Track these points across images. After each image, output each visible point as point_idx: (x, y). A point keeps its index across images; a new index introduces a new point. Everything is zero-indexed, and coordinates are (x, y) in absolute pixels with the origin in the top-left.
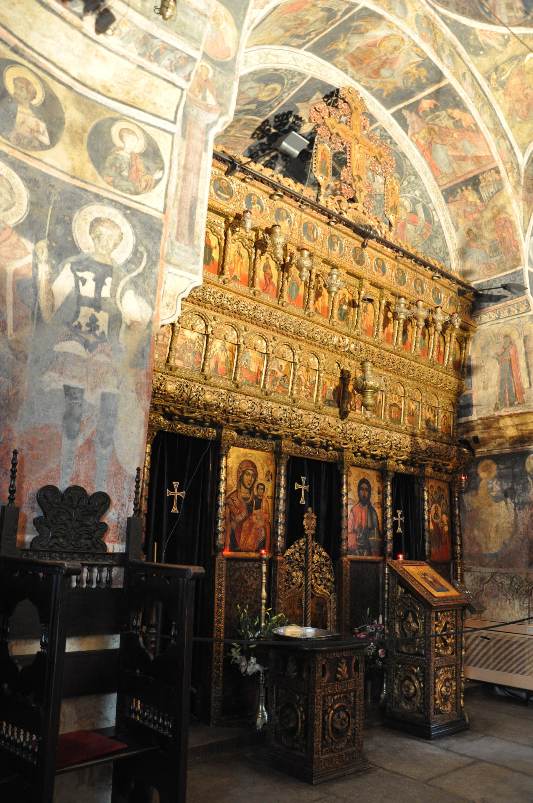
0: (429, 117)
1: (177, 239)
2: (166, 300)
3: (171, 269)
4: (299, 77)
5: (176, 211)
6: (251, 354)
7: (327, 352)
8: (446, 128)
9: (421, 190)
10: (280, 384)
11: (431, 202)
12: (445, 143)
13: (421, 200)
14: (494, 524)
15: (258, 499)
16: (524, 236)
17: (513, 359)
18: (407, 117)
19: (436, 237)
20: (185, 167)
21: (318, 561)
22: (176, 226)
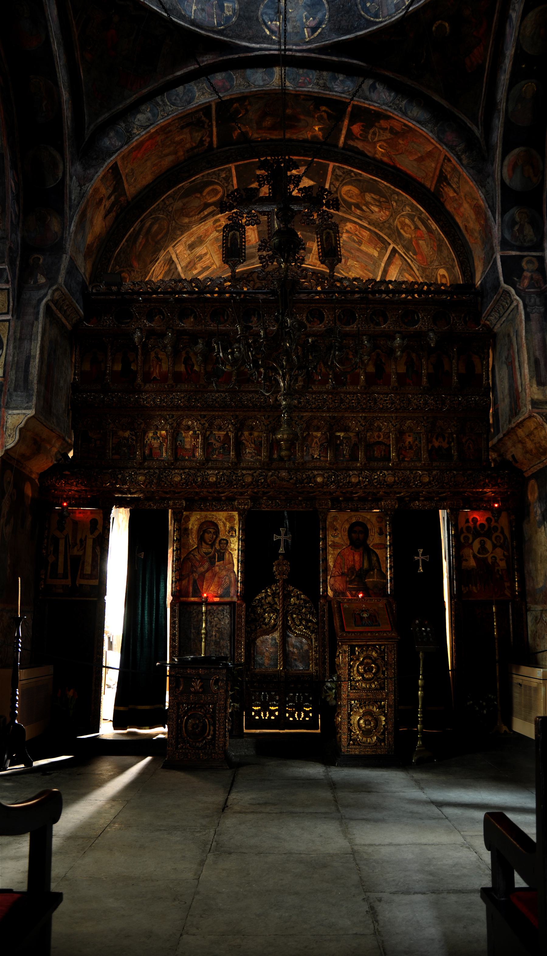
0: (369, 137)
1: (15, 390)
2: (9, 432)
3: (10, 412)
4: (225, 172)
5: (14, 372)
6: (184, 435)
8: (389, 139)
9: (408, 205)
10: (219, 453)
11: (423, 213)
13: (414, 213)
14: (539, 555)
15: (221, 553)
16: (495, 218)
18: (355, 145)
20: (20, 339)
21: (295, 604)
22: (14, 382)
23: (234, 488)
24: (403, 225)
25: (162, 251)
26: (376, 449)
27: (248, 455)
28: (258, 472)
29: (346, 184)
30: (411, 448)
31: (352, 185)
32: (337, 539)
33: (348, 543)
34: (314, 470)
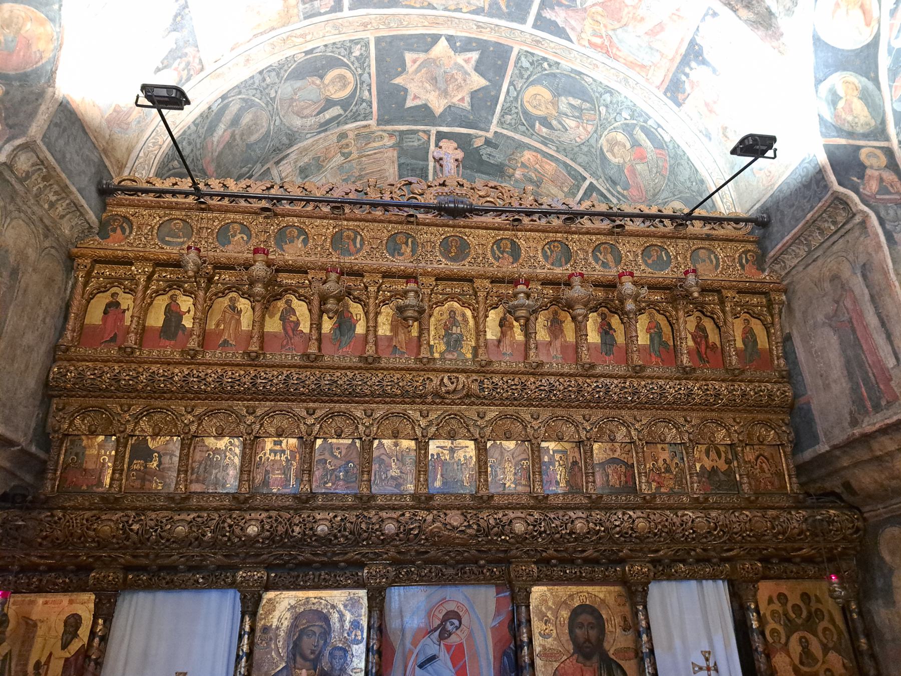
4: (359, 46)
7: (424, 407)
11: (650, 118)
12: (624, 21)
13: (635, 122)
17: (854, 316)
18: (553, 18)
19: (679, 164)
23: (363, 546)
24: (613, 144)
25: (259, 165)
26: (610, 472)
27: (391, 482)
28: (407, 515)
29: (532, 83)
30: (668, 470)
31: (542, 84)
32: (550, 642)
33: (571, 647)
34: (510, 509)
